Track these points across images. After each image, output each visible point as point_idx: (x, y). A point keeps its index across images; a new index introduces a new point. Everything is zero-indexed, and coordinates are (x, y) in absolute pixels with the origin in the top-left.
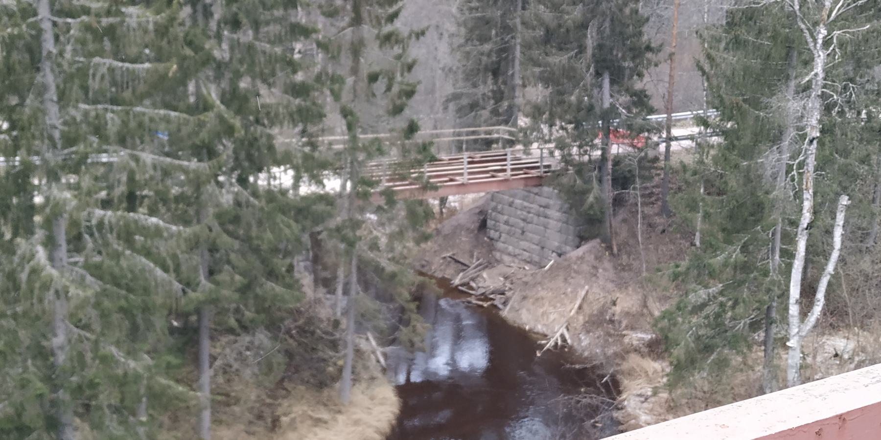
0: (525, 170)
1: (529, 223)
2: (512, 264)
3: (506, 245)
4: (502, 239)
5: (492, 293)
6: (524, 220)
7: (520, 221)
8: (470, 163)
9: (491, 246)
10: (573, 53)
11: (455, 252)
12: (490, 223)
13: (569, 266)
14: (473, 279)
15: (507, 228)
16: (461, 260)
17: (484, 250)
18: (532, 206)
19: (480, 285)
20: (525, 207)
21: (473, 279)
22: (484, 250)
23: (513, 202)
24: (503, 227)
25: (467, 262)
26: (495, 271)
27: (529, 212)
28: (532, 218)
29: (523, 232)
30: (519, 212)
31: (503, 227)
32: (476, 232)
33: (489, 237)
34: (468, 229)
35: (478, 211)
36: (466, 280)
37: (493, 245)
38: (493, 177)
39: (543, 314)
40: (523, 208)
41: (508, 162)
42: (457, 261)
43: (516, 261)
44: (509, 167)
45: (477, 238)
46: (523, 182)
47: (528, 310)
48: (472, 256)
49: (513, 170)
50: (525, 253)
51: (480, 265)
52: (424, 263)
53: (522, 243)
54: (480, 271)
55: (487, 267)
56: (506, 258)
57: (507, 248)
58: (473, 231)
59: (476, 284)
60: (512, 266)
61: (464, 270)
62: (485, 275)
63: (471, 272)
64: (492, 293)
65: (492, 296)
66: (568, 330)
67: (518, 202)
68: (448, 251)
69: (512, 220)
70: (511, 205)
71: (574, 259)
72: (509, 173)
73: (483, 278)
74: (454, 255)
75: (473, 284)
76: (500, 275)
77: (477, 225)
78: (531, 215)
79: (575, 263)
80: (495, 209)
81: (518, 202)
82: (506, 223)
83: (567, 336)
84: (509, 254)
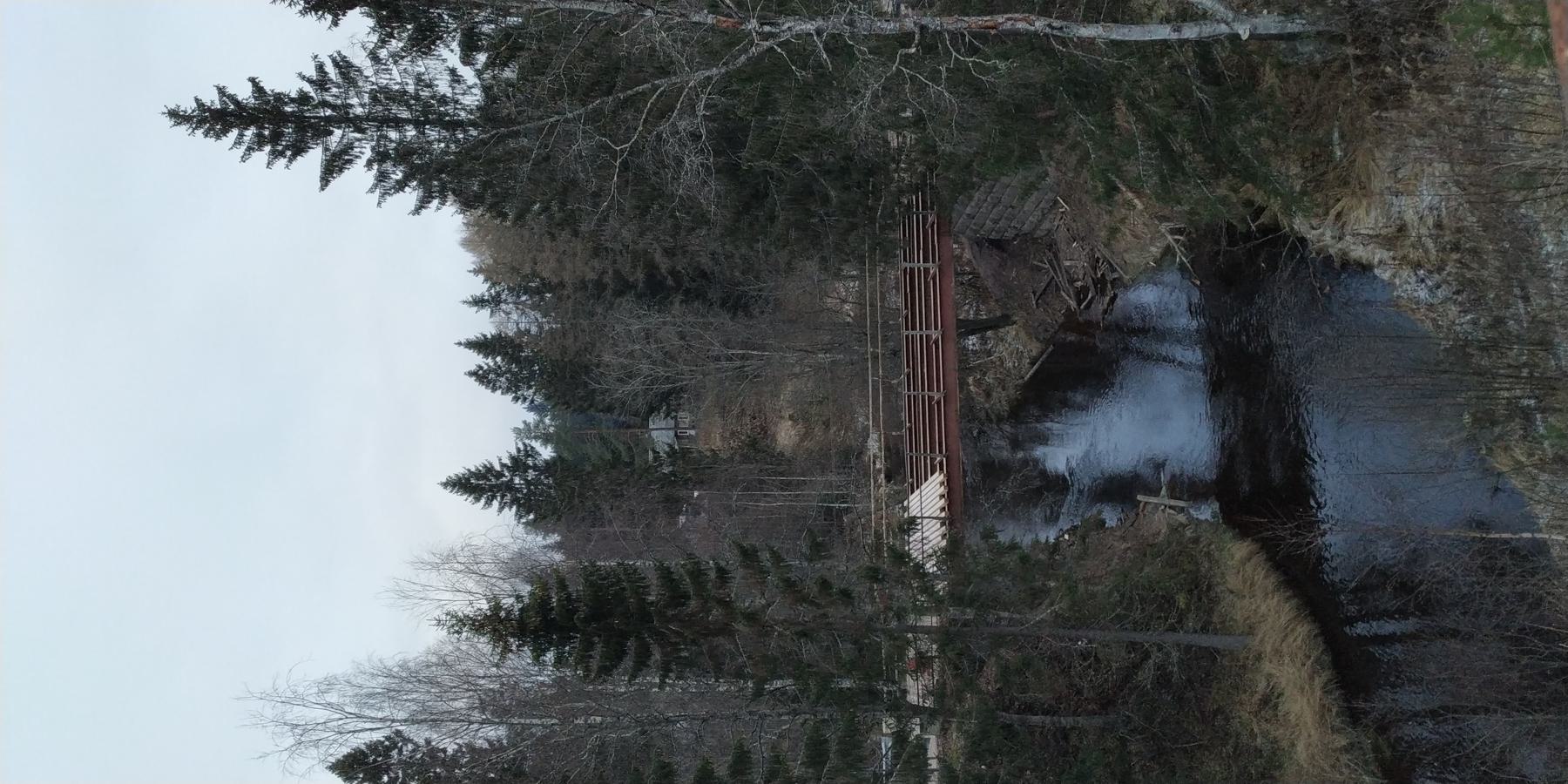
1: (999, 202)
2: (1056, 223)
3: (1028, 222)
4: (1018, 226)
5: (1095, 269)
7: (995, 210)
8: (914, 328)
9: (1028, 238)
11: (1030, 290)
12: (993, 236)
14: (1072, 281)
15: (1003, 220)
16: (1043, 285)
18: (976, 198)
19: (1081, 277)
20: (977, 205)
21: (1072, 281)
25: (1046, 279)
26: (1063, 246)
27: (986, 200)
28: (992, 198)
29: (1013, 207)
32: (1005, 255)
33: (1014, 239)
34: (1000, 266)
35: (975, 247)
37: (1026, 234)
38: (934, 278)
39: (1136, 237)
41: (915, 265)
42: (1045, 289)
48: (1039, 269)
49: (926, 260)
50: (1041, 206)
51: (1050, 262)
52: (1040, 329)
53: (1026, 208)
54: (1060, 268)
56: (1046, 225)
57: (1031, 222)
58: (1002, 258)
61: (1058, 289)
62: (1068, 263)
63: (1062, 280)
64: (1095, 269)
66: (1164, 219)
67: (968, 210)
70: (972, 217)
73: (1070, 267)
74: (1034, 293)
76: (1069, 244)
78: (989, 199)
79: (1065, 174)
80: (976, 232)
81: (968, 210)
83: (1171, 225)
84: (1040, 222)
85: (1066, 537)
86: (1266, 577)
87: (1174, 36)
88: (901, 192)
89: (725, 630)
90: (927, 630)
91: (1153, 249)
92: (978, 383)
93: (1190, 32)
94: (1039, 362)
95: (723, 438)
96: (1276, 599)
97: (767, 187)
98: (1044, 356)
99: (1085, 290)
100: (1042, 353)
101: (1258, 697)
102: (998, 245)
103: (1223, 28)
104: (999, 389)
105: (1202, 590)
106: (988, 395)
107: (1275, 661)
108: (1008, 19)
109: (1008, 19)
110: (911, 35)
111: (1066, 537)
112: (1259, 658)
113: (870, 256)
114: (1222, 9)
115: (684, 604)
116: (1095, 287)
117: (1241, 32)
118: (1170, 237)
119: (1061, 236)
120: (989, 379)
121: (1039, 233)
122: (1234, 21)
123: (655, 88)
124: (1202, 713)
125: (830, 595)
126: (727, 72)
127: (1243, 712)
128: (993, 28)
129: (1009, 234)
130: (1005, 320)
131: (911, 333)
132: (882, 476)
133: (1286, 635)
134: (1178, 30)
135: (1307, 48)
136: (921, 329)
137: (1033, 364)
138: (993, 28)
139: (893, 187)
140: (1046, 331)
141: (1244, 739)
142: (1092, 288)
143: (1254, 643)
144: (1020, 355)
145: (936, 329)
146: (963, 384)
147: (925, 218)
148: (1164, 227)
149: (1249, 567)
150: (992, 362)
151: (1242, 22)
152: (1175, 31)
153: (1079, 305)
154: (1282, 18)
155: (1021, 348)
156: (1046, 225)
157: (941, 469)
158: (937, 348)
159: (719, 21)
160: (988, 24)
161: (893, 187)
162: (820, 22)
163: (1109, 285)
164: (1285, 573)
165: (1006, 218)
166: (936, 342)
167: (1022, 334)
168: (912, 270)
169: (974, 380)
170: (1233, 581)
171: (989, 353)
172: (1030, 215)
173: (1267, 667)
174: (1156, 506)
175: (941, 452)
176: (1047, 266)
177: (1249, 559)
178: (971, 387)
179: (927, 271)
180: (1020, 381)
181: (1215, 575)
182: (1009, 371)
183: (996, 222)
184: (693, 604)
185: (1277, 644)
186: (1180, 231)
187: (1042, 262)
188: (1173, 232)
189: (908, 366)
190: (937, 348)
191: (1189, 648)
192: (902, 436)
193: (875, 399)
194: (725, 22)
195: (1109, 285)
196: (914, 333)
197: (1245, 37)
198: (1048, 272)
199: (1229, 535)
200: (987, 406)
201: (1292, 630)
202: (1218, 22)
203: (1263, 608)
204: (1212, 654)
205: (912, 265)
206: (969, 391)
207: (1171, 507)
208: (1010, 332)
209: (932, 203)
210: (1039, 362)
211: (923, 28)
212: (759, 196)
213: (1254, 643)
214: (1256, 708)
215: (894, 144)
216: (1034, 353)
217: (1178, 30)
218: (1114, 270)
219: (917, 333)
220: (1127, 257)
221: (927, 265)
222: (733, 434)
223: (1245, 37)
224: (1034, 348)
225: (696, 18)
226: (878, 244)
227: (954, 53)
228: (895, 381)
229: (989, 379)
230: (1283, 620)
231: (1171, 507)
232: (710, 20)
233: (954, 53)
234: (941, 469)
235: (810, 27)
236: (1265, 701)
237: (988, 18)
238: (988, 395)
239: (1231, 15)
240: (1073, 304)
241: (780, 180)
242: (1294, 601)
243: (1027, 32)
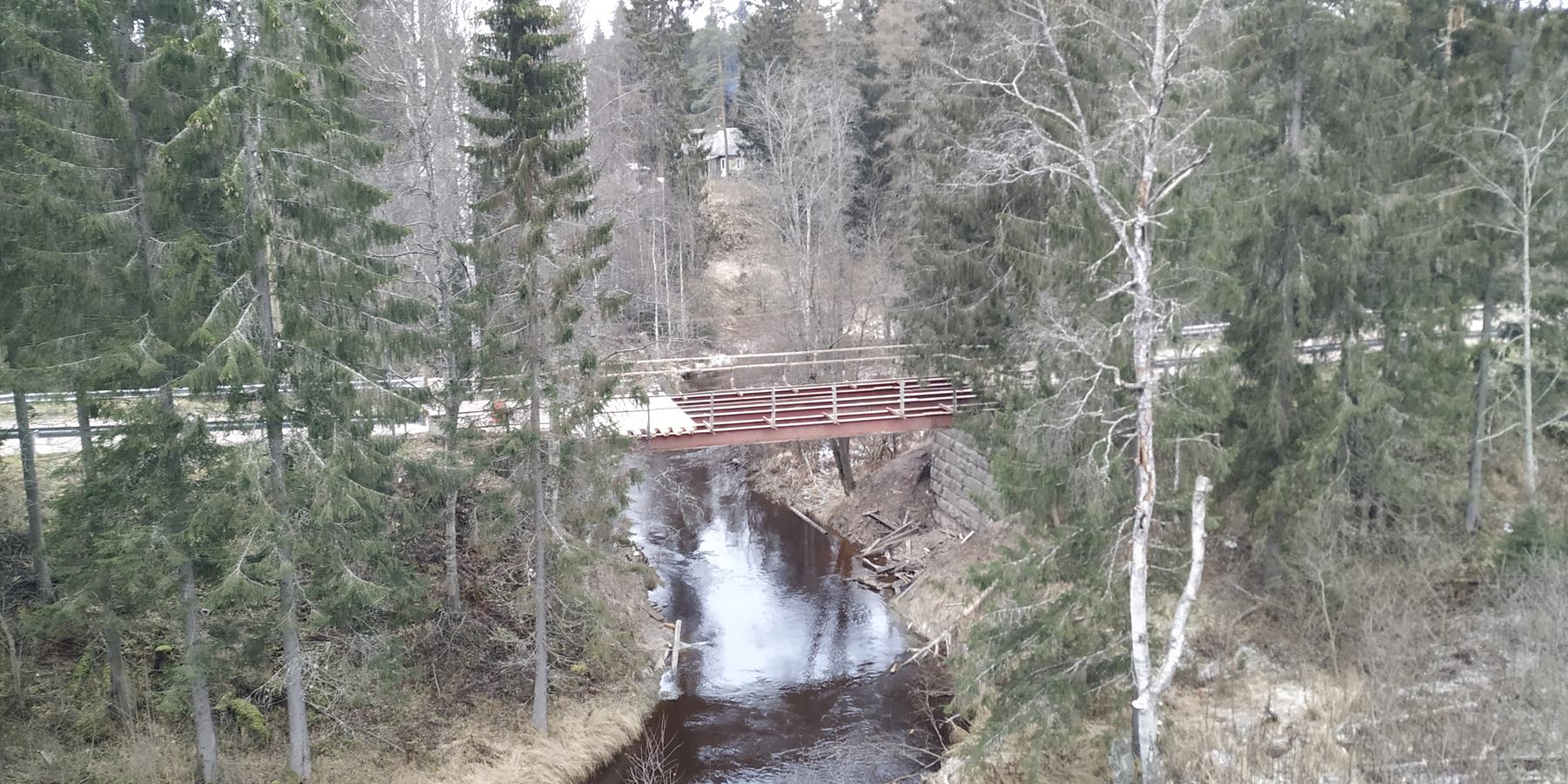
0: (942, 405)
2: (947, 531)
4: (944, 495)
6: (964, 470)
8: (839, 395)
9: (932, 504)
10: (981, 246)
12: (933, 471)
13: (987, 541)
15: (949, 479)
16: (885, 521)
17: (921, 508)
18: (971, 451)
21: (890, 549)
22: (921, 508)
23: (953, 445)
24: (946, 478)
26: (925, 538)
30: (959, 459)
31: (946, 478)
33: (931, 491)
35: (922, 453)
36: (881, 549)
38: (890, 413)
39: (937, 608)
40: (963, 454)
41: (902, 394)
43: (954, 526)
44: (902, 401)
45: (914, 490)
46: (929, 421)
47: (922, 600)
48: (901, 517)
49: (907, 404)
52: (842, 520)
53: (962, 501)
55: (916, 532)
56: (945, 521)
58: (912, 479)
59: (892, 554)
60: (944, 532)
61: (882, 535)
62: (908, 544)
63: (892, 539)
65: (897, 575)
66: (955, 634)
67: (958, 444)
68: (872, 506)
69: (954, 470)
70: (952, 448)
71: (997, 531)
72: (903, 409)
74: (877, 513)
75: (888, 556)
76: (927, 545)
77: (918, 473)
80: (937, 453)
81: (958, 444)
82: (947, 472)
83: (949, 642)
85: (637, 553)
86: (606, 746)
87: (1135, 636)
88: (975, 378)
89: (523, 214)
90: (535, 419)
91: (924, 626)
92: (786, 462)
93: (1140, 652)
94: (808, 520)
95: (720, 206)
96: (584, 756)
97: (978, 241)
98: (815, 525)
99: (882, 562)
100: (818, 523)
101: (487, 743)
102: (925, 475)
103: (1142, 683)
104: (781, 483)
105: (592, 684)
106: (774, 472)
107: (524, 758)
108: (1150, 476)
109: (1150, 476)
110: (1133, 379)
111: (637, 553)
112: (526, 742)
113: (909, 348)
114: (1162, 681)
115: (547, 168)
116: (886, 571)
117: (1140, 699)
118: (936, 641)
119: (934, 536)
120: (791, 472)
121: (937, 514)
122: (1151, 693)
123: (1076, 120)
124: (468, 691)
125: (565, 320)
126: (1093, 194)
127: (469, 730)
128: (1141, 460)
129: (936, 486)
130: (850, 486)
131: (834, 392)
132: (689, 370)
133: (549, 767)
134: (1141, 640)
135: (1125, 763)
136: (839, 402)
137: (807, 514)
138: (1141, 460)
139: (980, 369)
140: (841, 526)
141: (445, 733)
142: (884, 569)
143: (541, 737)
144: (815, 501)
145: (839, 417)
146: (784, 446)
147: (950, 402)
148: (946, 635)
149: (615, 730)
150: (808, 474)
151: (1150, 701)
152: (1140, 637)
153: (867, 557)
154: (1154, 739)
155: (822, 502)
156: (945, 521)
157: (699, 428)
158: (820, 419)
159: (1145, 183)
160: (1145, 456)
161: (980, 369)
162: (1145, 287)
163: (887, 585)
164: (611, 764)
165: (951, 483)
166: (825, 418)
167: (836, 503)
168: (897, 391)
169: (788, 458)
170: (600, 715)
171: (816, 471)
172: (954, 504)
173: (518, 751)
174: (671, 639)
175: (716, 426)
176: (905, 525)
177: (623, 730)
178: (781, 455)
179: (897, 405)
180: (789, 503)
181: (604, 696)
182: (799, 491)
183: (947, 472)
184: (548, 179)
185: (541, 759)
186: (943, 651)
187: (909, 518)
188: (942, 644)
189: (801, 391)
190: (820, 419)
191: (533, 675)
192: (729, 387)
193: (767, 360)
194: (1144, 190)
195: (887, 585)
196: (834, 396)
197: (1136, 704)
198: (899, 525)
199: (646, 710)
200: (764, 471)
201: (556, 774)
202: (1149, 678)
203: (575, 745)
204: (528, 699)
205: (902, 390)
206: (778, 453)
207: (671, 653)
208: (838, 490)
209: (965, 408)
210: (808, 520)
211: (1141, 391)
212: (968, 234)
213: (541, 737)
214: (477, 740)
215: (1023, 368)
216: (818, 515)
217: (1141, 640)
218: (902, 589)
219: (834, 399)
220: (916, 601)
221: (902, 406)
222: (724, 216)
223: (1136, 704)
224: (823, 515)
225: (1148, 160)
226: (922, 357)
227: (1115, 423)
228: (784, 378)
229: (791, 472)
230: (565, 764)
231: (671, 653)
232: (1147, 175)
233: (1115, 423)
234: (699, 428)
235: (1141, 277)
236: (484, 751)
237: (1151, 455)
238: (774, 472)
239: (1156, 690)
240: (868, 551)
241: (985, 254)
242: (583, 774)
243: (1136, 494)
